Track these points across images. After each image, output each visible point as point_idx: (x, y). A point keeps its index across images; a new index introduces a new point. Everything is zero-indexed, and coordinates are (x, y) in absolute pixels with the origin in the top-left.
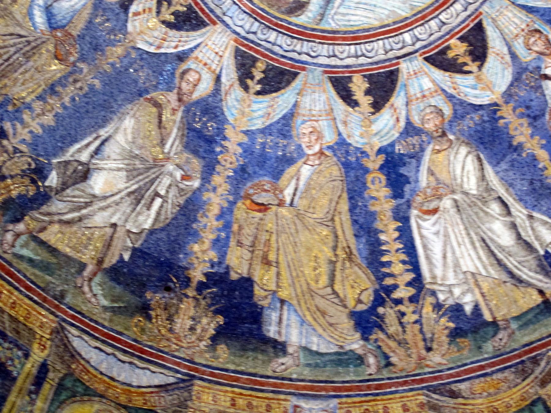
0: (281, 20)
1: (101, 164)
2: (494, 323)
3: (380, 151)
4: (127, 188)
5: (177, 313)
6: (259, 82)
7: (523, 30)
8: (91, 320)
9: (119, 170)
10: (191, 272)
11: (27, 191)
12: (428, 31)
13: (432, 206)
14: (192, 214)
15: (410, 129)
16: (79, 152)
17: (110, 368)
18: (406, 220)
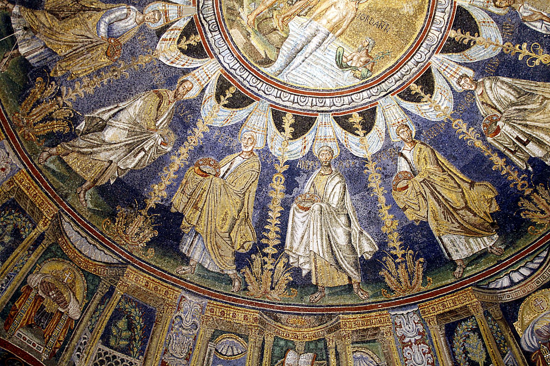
2: (316, 286)
3: (286, 163)
4: (125, 141)
5: (132, 222)
6: (228, 99)
7: (399, 123)
8: (79, 214)
9: (124, 129)
10: (148, 201)
11: (64, 130)
12: (342, 102)
13: (307, 205)
14: (161, 166)
16: (103, 113)
18: (289, 208)
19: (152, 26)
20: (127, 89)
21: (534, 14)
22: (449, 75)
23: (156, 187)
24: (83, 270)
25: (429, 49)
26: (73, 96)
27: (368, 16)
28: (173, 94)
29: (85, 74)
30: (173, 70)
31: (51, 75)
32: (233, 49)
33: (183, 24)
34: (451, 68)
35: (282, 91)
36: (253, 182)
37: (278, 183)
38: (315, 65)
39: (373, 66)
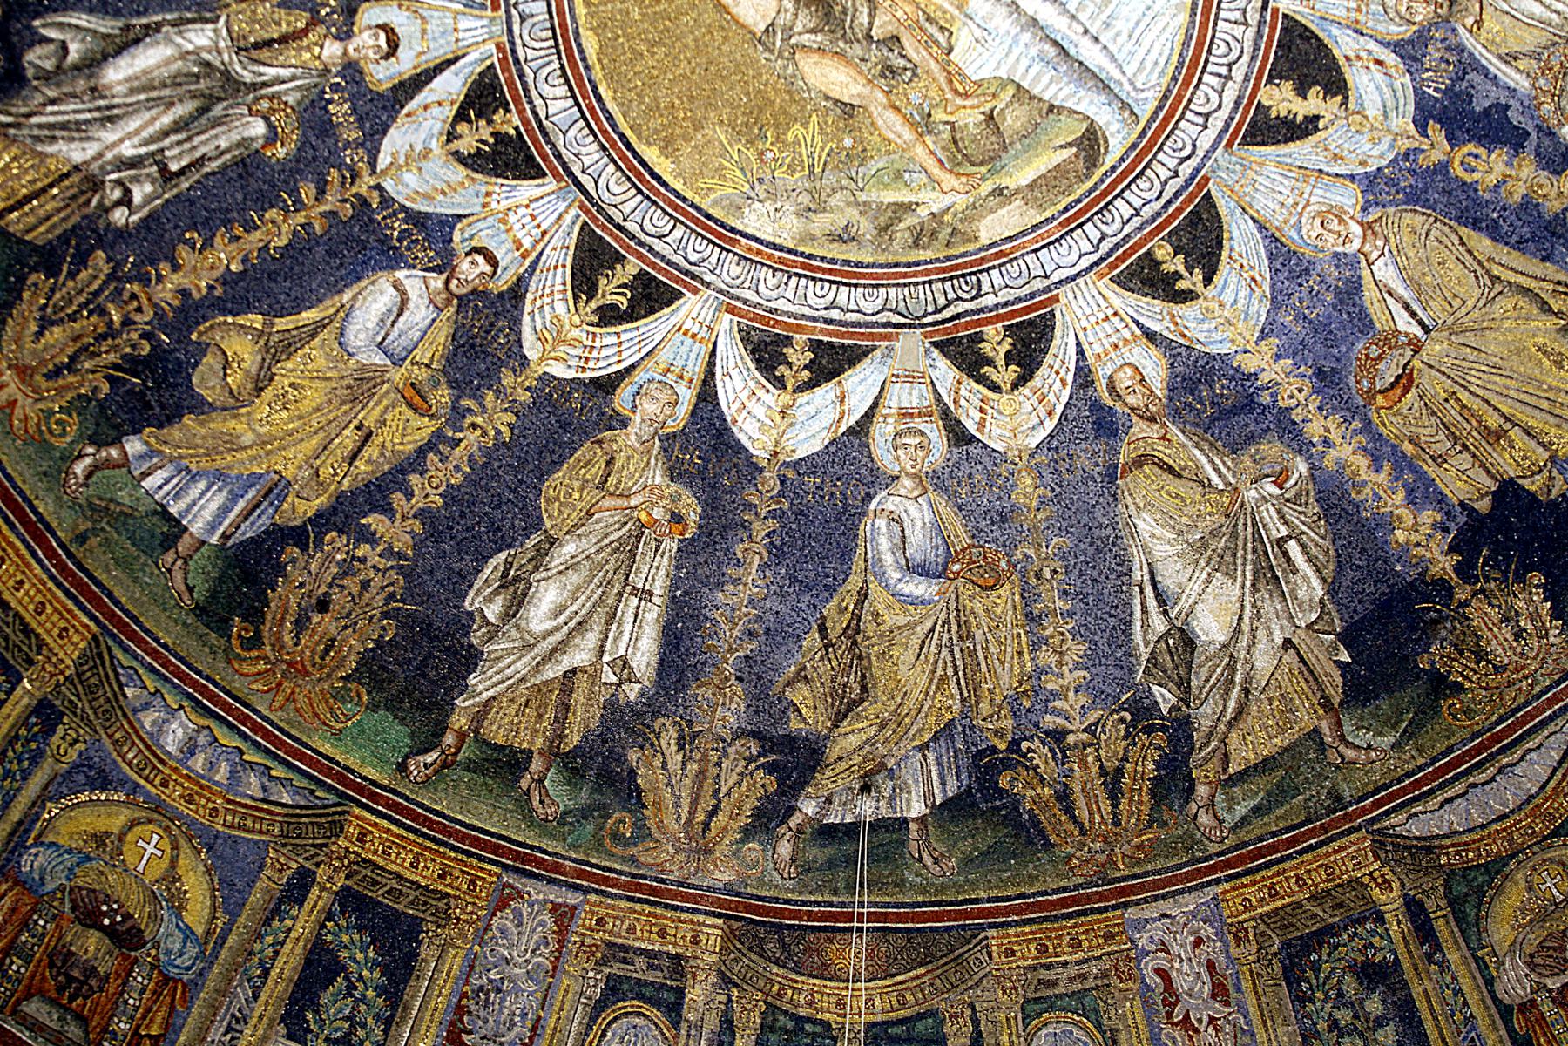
1: (1184, 604)
3: (1421, 126)
5: (1479, 638)
8: (1399, 781)
9: (1208, 581)
11: (1159, 748)
15: (1410, 51)
17: (1484, 807)
19: (937, 455)
20: (1098, 551)
23: (1400, 535)
24: (1555, 834)
26: (1076, 701)
28: (1143, 425)
29: (1027, 657)
30: (1072, 414)
31: (1003, 747)
32: (1039, 238)
33: (945, 372)
35: (1187, 107)
36: (1462, 244)
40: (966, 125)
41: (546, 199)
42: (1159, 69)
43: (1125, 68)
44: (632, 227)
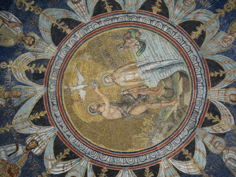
0: (191, 77)
3: (216, 13)
6: (218, 72)
12: (158, 24)
19: (223, 142)
21: (14, 27)
22: (84, 7)
25: (87, 28)
27: (111, 64)
33: (208, 129)
34: (80, 11)
35: (186, 53)
37: (230, 6)
38: (158, 55)
39: (126, 34)
40: (164, 93)
41: (124, 174)
42: (176, 53)
43: (172, 59)
44: (140, 163)
